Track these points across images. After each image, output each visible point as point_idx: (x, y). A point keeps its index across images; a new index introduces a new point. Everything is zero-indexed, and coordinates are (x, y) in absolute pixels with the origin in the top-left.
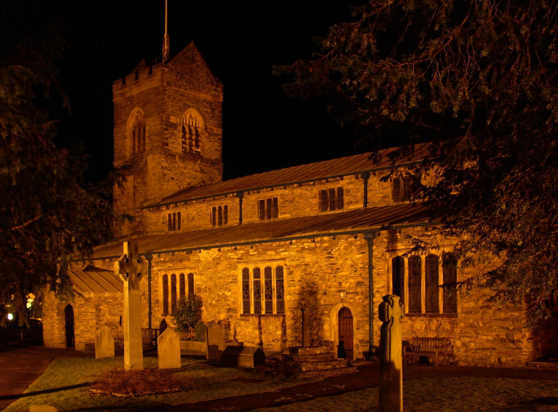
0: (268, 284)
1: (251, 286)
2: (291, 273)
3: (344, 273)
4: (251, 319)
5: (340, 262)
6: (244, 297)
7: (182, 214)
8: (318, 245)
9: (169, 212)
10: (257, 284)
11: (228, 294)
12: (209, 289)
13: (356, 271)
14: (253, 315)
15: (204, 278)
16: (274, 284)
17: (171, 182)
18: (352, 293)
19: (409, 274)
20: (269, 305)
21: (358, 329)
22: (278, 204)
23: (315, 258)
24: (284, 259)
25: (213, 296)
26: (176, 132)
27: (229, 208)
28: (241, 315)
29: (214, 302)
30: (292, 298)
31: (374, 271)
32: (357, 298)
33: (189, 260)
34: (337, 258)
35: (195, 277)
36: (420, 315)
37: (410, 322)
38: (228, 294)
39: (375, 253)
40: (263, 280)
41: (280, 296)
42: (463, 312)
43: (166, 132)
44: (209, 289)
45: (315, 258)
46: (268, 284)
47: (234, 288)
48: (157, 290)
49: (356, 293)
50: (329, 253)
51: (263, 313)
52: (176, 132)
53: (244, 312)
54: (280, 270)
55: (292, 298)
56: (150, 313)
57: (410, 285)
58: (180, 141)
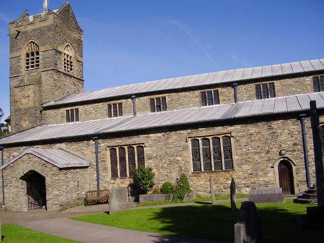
0: (217, 150)
3: (283, 139)
4: (202, 175)
5: (279, 131)
6: (193, 160)
9: (67, 109)
11: (180, 159)
12: (160, 156)
13: (292, 137)
14: (204, 172)
15: (154, 148)
18: (291, 151)
21: (297, 174)
22: (167, 101)
23: (257, 130)
27: (123, 105)
28: (192, 173)
29: (165, 165)
30: (239, 158)
34: (276, 129)
38: (178, 158)
43: (56, 56)
44: (160, 156)
45: (257, 130)
46: (217, 150)
47: (184, 153)
48: (105, 160)
51: (213, 170)
53: (194, 171)
54: (228, 138)
55: (239, 158)
56: (98, 179)
58: (63, 63)
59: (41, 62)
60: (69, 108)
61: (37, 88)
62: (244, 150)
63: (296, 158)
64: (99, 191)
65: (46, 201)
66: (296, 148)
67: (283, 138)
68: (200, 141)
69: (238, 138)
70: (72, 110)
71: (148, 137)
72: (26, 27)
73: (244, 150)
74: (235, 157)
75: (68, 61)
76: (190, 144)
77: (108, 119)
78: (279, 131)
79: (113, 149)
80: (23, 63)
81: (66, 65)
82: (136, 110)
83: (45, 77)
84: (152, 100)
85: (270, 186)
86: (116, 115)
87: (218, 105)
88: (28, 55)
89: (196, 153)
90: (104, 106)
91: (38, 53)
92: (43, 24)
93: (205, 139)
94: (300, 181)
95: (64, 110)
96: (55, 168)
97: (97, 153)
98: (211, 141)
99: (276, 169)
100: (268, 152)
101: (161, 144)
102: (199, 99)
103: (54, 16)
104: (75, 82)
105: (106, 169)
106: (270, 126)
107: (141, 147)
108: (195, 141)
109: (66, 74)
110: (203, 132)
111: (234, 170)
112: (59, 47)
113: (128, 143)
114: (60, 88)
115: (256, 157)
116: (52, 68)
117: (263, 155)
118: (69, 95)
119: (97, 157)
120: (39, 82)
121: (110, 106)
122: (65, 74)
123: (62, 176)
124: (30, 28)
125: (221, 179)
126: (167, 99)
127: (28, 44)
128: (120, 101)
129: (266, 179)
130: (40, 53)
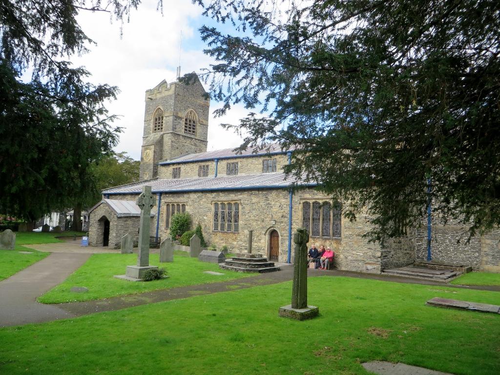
1: (220, 214)
2: (243, 208)
7: (181, 169)
8: (260, 192)
10: (223, 212)
11: (205, 218)
15: (192, 207)
16: (233, 214)
17: (177, 151)
19: (313, 213)
20: (229, 226)
21: (282, 243)
24: (240, 200)
25: (196, 219)
26: (181, 122)
27: (210, 167)
31: (293, 209)
32: (282, 224)
33: (184, 197)
35: (186, 207)
36: (318, 238)
37: (313, 241)
38: (205, 218)
39: (293, 200)
40: (226, 211)
41: (236, 221)
42: (346, 237)
49: (282, 222)
50: (267, 198)
52: (181, 122)
54: (237, 205)
57: (313, 219)
59: (164, 126)
60: (175, 167)
61: (158, 148)
62: (247, 216)
63: (284, 229)
64: (157, 238)
65: (108, 240)
66: (283, 219)
67: (275, 209)
68: (220, 205)
69: (244, 206)
70: (176, 168)
71: (189, 198)
72: (156, 95)
73: (247, 216)
74: (241, 222)
75: (190, 125)
76: (213, 207)
77: (197, 177)
78: (273, 203)
79: (168, 205)
80: (152, 126)
81: (188, 129)
82: (218, 172)
83: (167, 139)
84: (228, 164)
85: (261, 251)
86: (204, 176)
87: (273, 173)
88: (156, 119)
89: (216, 214)
90: (196, 167)
91: (162, 117)
92: (167, 93)
93: (223, 204)
94: (282, 251)
95: (171, 168)
96: (115, 216)
97: (159, 207)
98: (220, 205)
99: (267, 237)
100: (263, 221)
101: (196, 205)
102: (261, 166)
103: (176, 87)
104: (197, 143)
105: (162, 221)
106: (267, 198)
107: (183, 205)
108: (216, 204)
109: (185, 136)
110: (223, 197)
111: (239, 233)
112: (179, 113)
113: (177, 201)
114: (177, 148)
115: (254, 223)
116: (171, 131)
117: (259, 223)
118: (188, 153)
119: (159, 210)
120: (160, 143)
121: (200, 166)
122: (183, 136)
123: (121, 223)
124: (159, 96)
125: (230, 240)
126: (239, 164)
127: (157, 110)
128: (207, 163)
129: (260, 244)
130: (164, 118)
